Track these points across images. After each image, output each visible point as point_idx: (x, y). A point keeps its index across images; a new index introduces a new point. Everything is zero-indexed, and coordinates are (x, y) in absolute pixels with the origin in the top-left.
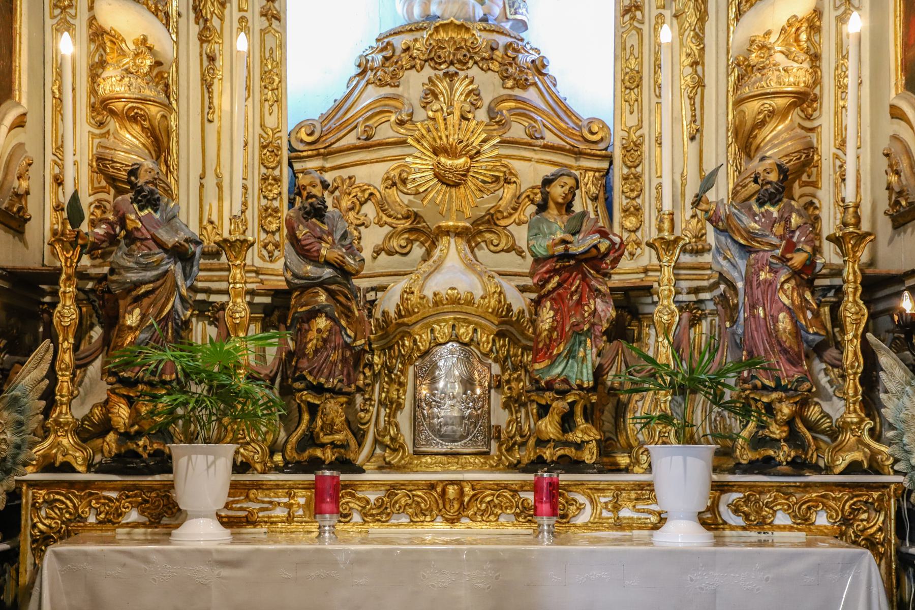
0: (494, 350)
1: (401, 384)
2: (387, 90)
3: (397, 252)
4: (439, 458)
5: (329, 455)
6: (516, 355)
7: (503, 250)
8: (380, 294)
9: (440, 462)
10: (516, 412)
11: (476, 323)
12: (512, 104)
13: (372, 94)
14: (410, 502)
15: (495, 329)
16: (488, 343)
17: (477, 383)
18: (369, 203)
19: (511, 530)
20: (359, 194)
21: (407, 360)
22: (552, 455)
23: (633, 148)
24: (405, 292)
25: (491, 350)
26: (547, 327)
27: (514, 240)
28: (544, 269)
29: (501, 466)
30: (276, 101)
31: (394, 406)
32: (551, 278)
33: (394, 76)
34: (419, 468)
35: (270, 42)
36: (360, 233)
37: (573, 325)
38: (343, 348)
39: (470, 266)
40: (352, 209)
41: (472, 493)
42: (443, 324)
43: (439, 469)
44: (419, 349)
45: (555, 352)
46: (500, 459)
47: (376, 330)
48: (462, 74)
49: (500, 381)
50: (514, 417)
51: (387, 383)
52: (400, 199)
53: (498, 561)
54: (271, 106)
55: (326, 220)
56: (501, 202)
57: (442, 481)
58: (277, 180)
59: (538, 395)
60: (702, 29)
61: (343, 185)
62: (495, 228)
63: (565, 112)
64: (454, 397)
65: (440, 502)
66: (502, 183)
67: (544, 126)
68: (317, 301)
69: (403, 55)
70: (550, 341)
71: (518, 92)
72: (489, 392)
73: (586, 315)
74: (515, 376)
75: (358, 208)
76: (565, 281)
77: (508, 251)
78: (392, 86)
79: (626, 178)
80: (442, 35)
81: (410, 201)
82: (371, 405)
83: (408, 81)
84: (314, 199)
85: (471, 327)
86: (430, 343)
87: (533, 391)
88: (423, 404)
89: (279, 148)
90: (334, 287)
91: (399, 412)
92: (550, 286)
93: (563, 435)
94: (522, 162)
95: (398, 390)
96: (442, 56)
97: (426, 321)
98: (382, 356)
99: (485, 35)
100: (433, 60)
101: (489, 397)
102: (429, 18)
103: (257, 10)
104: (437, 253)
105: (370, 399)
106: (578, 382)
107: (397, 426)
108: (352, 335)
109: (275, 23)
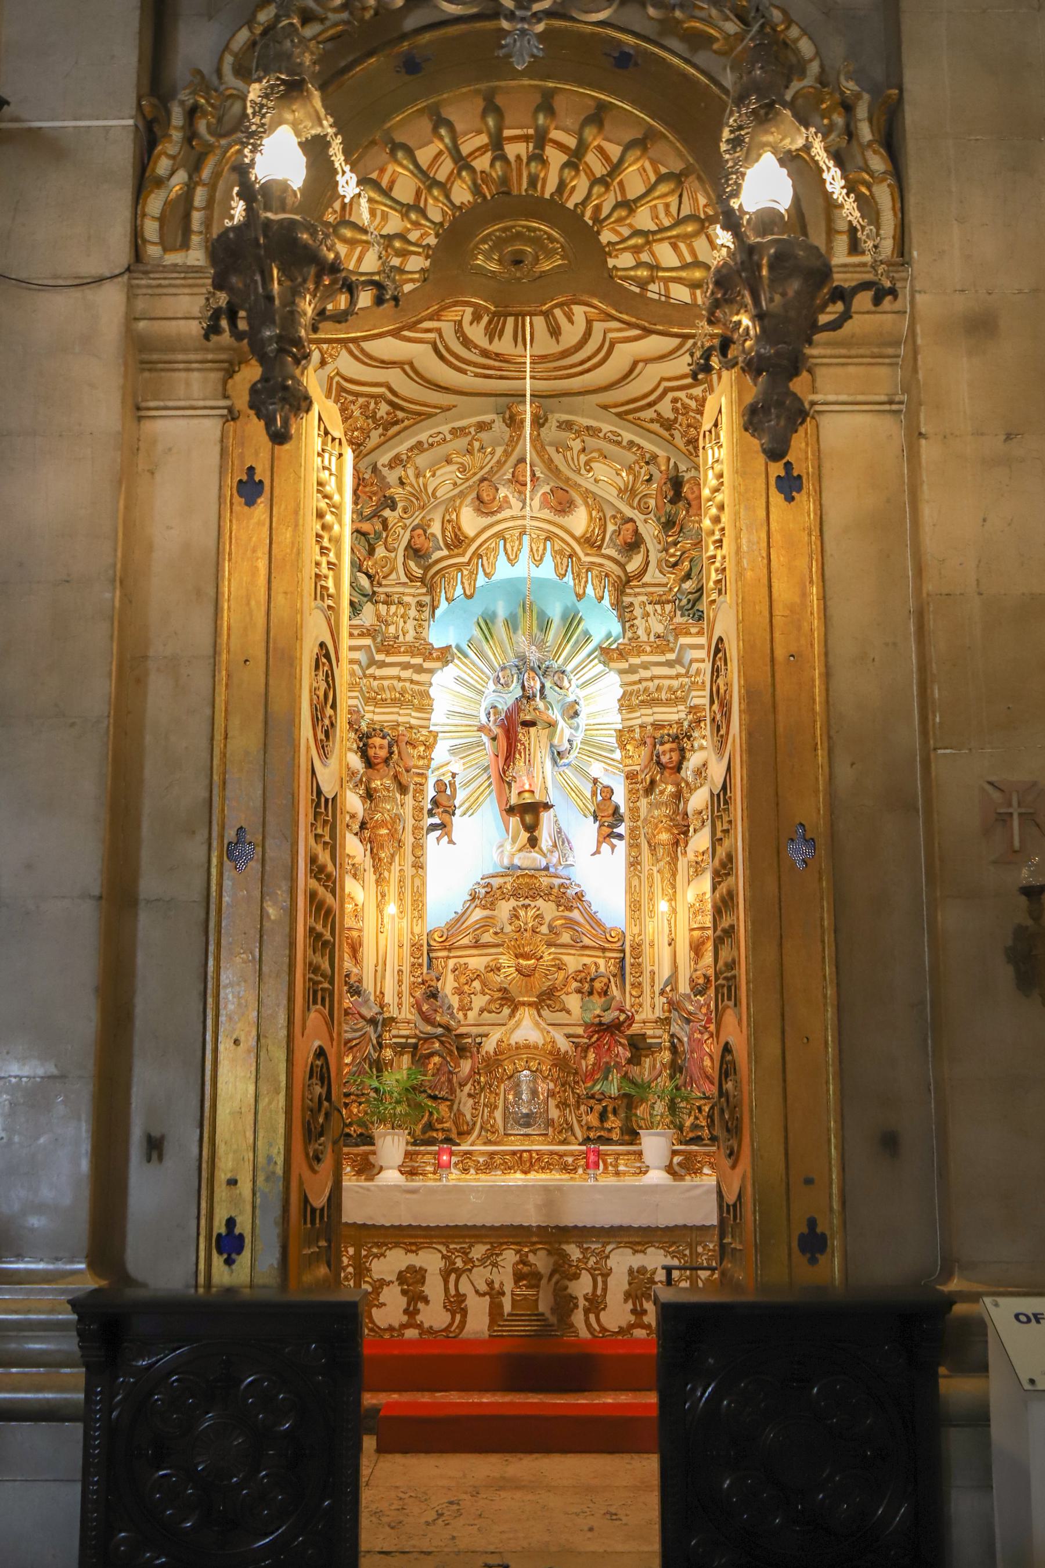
1: (497, 1094)
5: (440, 1136)
8: (484, 1039)
12: (563, 921)
13: (478, 914)
19: (558, 1176)
21: (501, 1080)
23: (637, 947)
33: (492, 903)
35: (417, 882)
39: (537, 1024)
48: (533, 904)
52: (498, 979)
53: (546, 1189)
58: (421, 965)
60: (675, 880)
71: (567, 913)
77: (561, 1011)
79: (632, 965)
89: (422, 946)
99: (546, 879)
100: (515, 895)
102: (513, 865)
103: (410, 864)
104: (518, 1015)
109: (420, 870)
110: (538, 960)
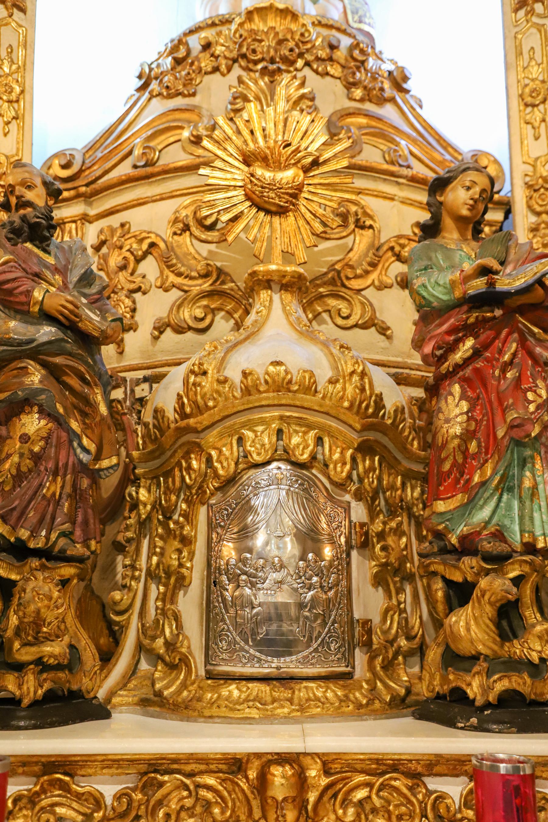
0: (355, 477)
2: (179, 102)
3: (190, 328)
4: (254, 686)
6: (392, 487)
7: (356, 326)
9: (257, 699)
10: (397, 593)
11: (322, 428)
12: (363, 121)
14: (188, 802)
15: (356, 439)
16: (344, 464)
17: (324, 538)
18: (150, 258)
20: (135, 246)
22: (486, 690)
24: (192, 372)
25: (349, 477)
26: (458, 430)
27: (374, 311)
28: (445, 327)
29: (377, 705)
30: (15, 118)
31: (173, 580)
32: (459, 341)
33: (188, 82)
34: (214, 711)
36: (134, 302)
37: (512, 427)
38: (75, 473)
40: (123, 268)
41: (324, 781)
42: (260, 428)
43: (254, 713)
44: (216, 476)
45: (476, 479)
46: (373, 688)
47: (144, 442)
49: (367, 534)
50: (394, 602)
51: (161, 538)
54: (8, 123)
55: (52, 248)
56: (351, 255)
57: (258, 755)
59: (445, 563)
61: (112, 237)
62: (343, 292)
63: (438, 141)
64: (282, 566)
65: (255, 804)
66: (352, 226)
67: (411, 153)
68: (22, 383)
69: (201, 55)
70: (465, 458)
71: (368, 106)
72: (349, 555)
73: (532, 408)
74: (393, 524)
75: (132, 265)
76: (486, 346)
77: (364, 326)
78: (184, 96)
80: (258, 25)
81: (210, 252)
82: (133, 578)
83: (209, 89)
84: (29, 210)
85: (312, 434)
86: (237, 464)
87: (434, 554)
88: (224, 578)
90: (58, 360)
91: (181, 593)
92: (458, 356)
93: (502, 646)
94: (380, 201)
95: (180, 551)
96: (259, 49)
97: (228, 423)
98: (153, 488)
101: (349, 564)
105: (133, 567)
106: (527, 538)
107: (177, 618)
108: (92, 447)
110: (306, 170)
